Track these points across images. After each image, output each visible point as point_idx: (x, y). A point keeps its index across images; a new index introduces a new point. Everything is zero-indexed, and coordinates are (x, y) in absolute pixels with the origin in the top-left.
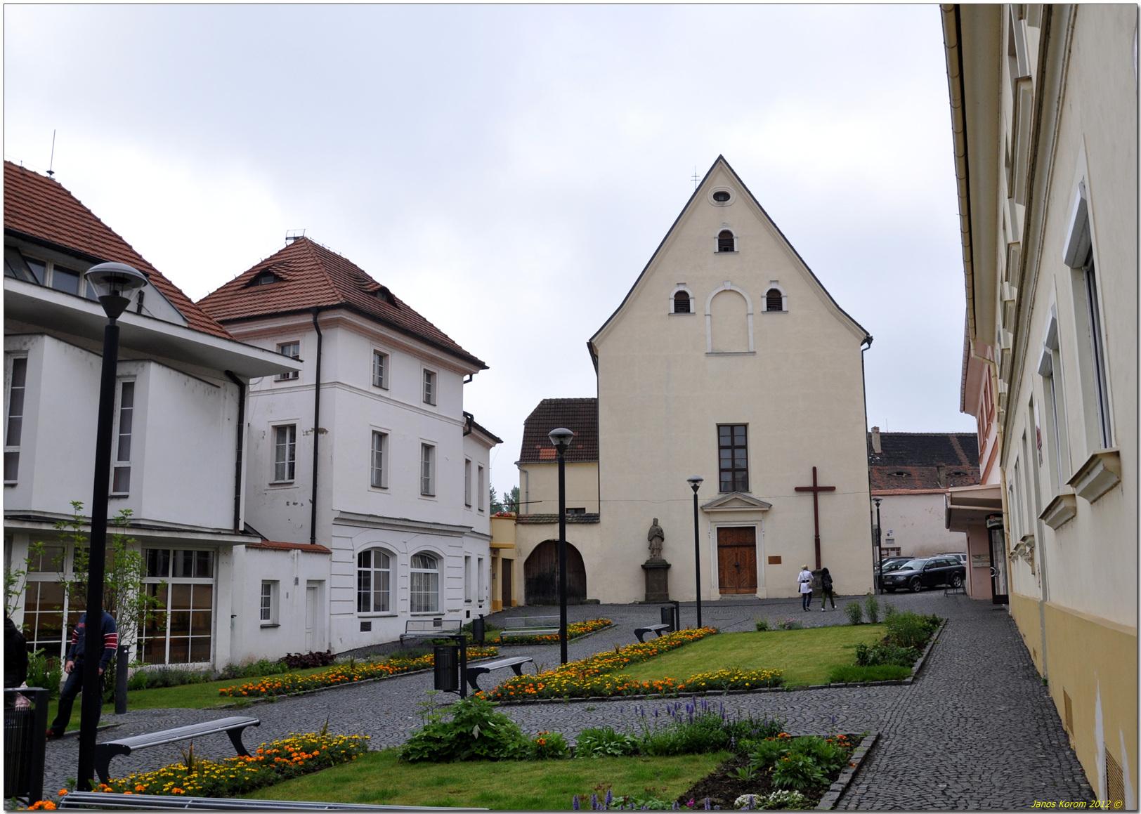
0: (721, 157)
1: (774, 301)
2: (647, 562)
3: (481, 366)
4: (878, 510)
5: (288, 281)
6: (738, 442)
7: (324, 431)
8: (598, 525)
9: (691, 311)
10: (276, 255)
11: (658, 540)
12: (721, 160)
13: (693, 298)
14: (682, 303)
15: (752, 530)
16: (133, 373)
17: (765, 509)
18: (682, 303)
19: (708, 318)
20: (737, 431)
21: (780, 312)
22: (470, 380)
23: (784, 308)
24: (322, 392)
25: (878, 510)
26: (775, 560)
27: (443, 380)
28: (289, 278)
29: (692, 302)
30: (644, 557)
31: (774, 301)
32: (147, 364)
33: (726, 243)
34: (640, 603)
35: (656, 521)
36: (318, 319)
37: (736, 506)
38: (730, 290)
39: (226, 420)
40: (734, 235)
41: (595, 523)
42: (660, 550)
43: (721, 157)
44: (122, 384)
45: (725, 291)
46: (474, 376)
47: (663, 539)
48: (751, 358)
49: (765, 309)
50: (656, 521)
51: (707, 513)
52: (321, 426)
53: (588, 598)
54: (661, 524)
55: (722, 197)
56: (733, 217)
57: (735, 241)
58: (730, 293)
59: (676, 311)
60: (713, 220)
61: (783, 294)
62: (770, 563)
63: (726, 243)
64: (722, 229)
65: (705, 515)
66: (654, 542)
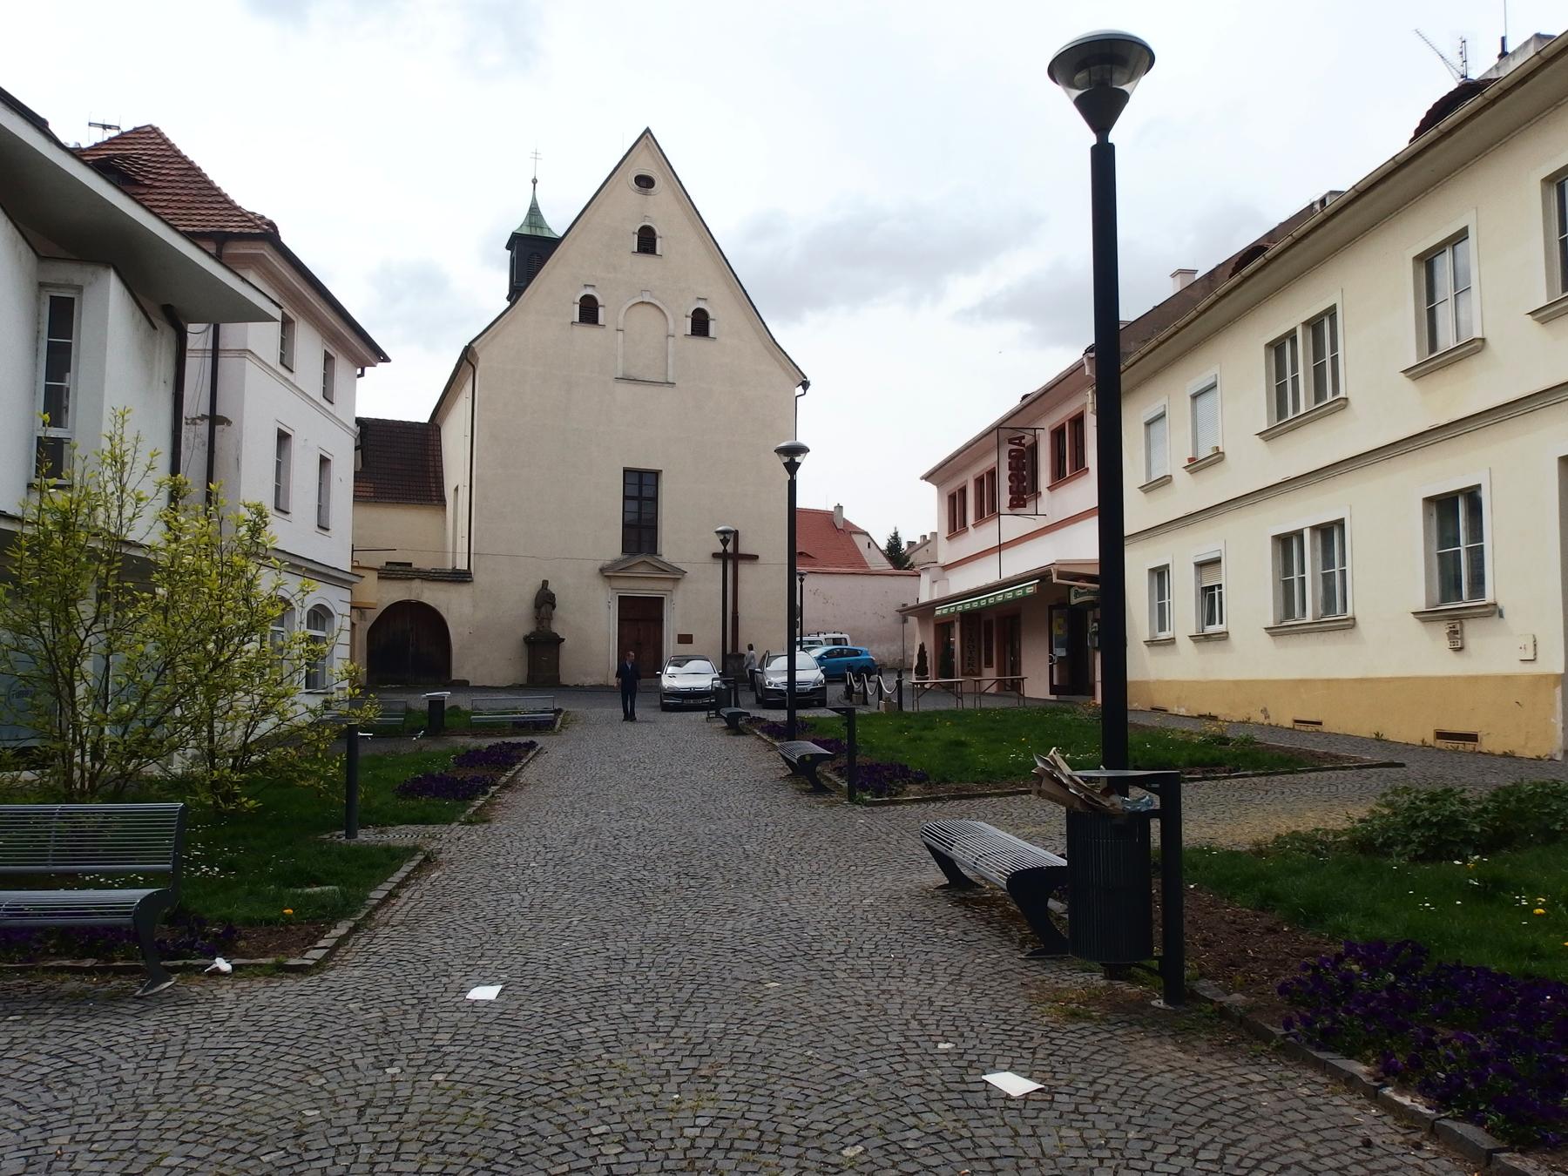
0: (648, 131)
1: (700, 324)
2: (532, 634)
3: (386, 359)
4: (801, 586)
5: (146, 186)
6: (647, 492)
7: (225, 421)
8: (470, 586)
9: (600, 323)
10: (104, 143)
11: (550, 607)
12: (648, 134)
13: (603, 306)
14: (589, 311)
15: (658, 602)
16: (77, 282)
17: (675, 575)
18: (589, 311)
19: (620, 333)
20: (646, 479)
21: (706, 338)
22: (362, 375)
23: (712, 334)
24: (221, 361)
25: (801, 586)
26: (685, 639)
27: (342, 366)
28: (147, 182)
29: (601, 311)
30: (526, 628)
31: (700, 324)
32: (101, 271)
33: (647, 241)
34: (521, 685)
35: (545, 583)
36: (224, 251)
37: (642, 570)
38: (649, 303)
39: (162, 384)
40: (658, 233)
41: (467, 582)
42: (550, 618)
43: (648, 131)
44: (48, 299)
45: (643, 302)
46: (367, 369)
47: (554, 607)
48: (667, 390)
49: (689, 332)
50: (545, 583)
51: (608, 577)
52: (220, 412)
53: (453, 678)
54: (552, 587)
55: (645, 182)
56: (657, 210)
57: (658, 241)
58: (648, 307)
59: (582, 320)
60: (632, 210)
61: (711, 315)
62: (679, 642)
63: (647, 241)
64: (643, 224)
65: (606, 580)
66: (543, 609)
